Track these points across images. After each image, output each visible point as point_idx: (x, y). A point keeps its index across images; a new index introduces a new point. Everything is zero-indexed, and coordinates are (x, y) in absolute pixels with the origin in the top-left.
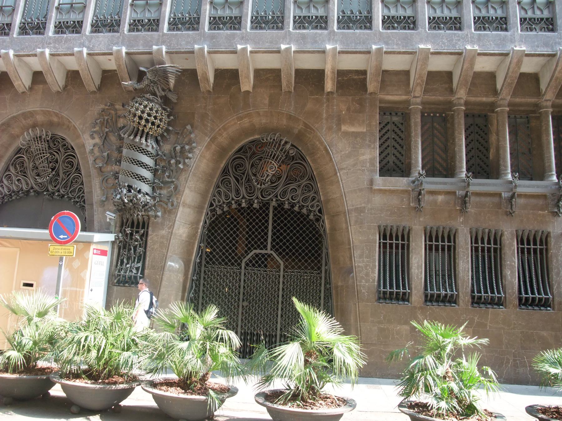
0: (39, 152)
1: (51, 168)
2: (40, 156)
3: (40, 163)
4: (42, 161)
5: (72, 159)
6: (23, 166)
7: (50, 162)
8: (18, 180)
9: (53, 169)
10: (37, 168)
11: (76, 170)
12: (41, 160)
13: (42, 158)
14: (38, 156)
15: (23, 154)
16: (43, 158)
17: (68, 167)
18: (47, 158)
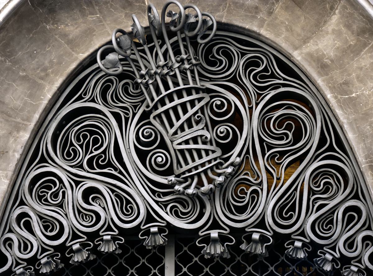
0: (164, 93)
1: (218, 144)
2: (177, 101)
3: (182, 128)
4: (189, 121)
5: (290, 107)
6: (96, 141)
7: (214, 123)
8: (88, 193)
9: (227, 148)
10: (163, 145)
11: (322, 141)
12: (183, 118)
13: (185, 111)
14: (169, 105)
15: (93, 101)
16: (191, 112)
17: (281, 139)
18: (202, 109)
